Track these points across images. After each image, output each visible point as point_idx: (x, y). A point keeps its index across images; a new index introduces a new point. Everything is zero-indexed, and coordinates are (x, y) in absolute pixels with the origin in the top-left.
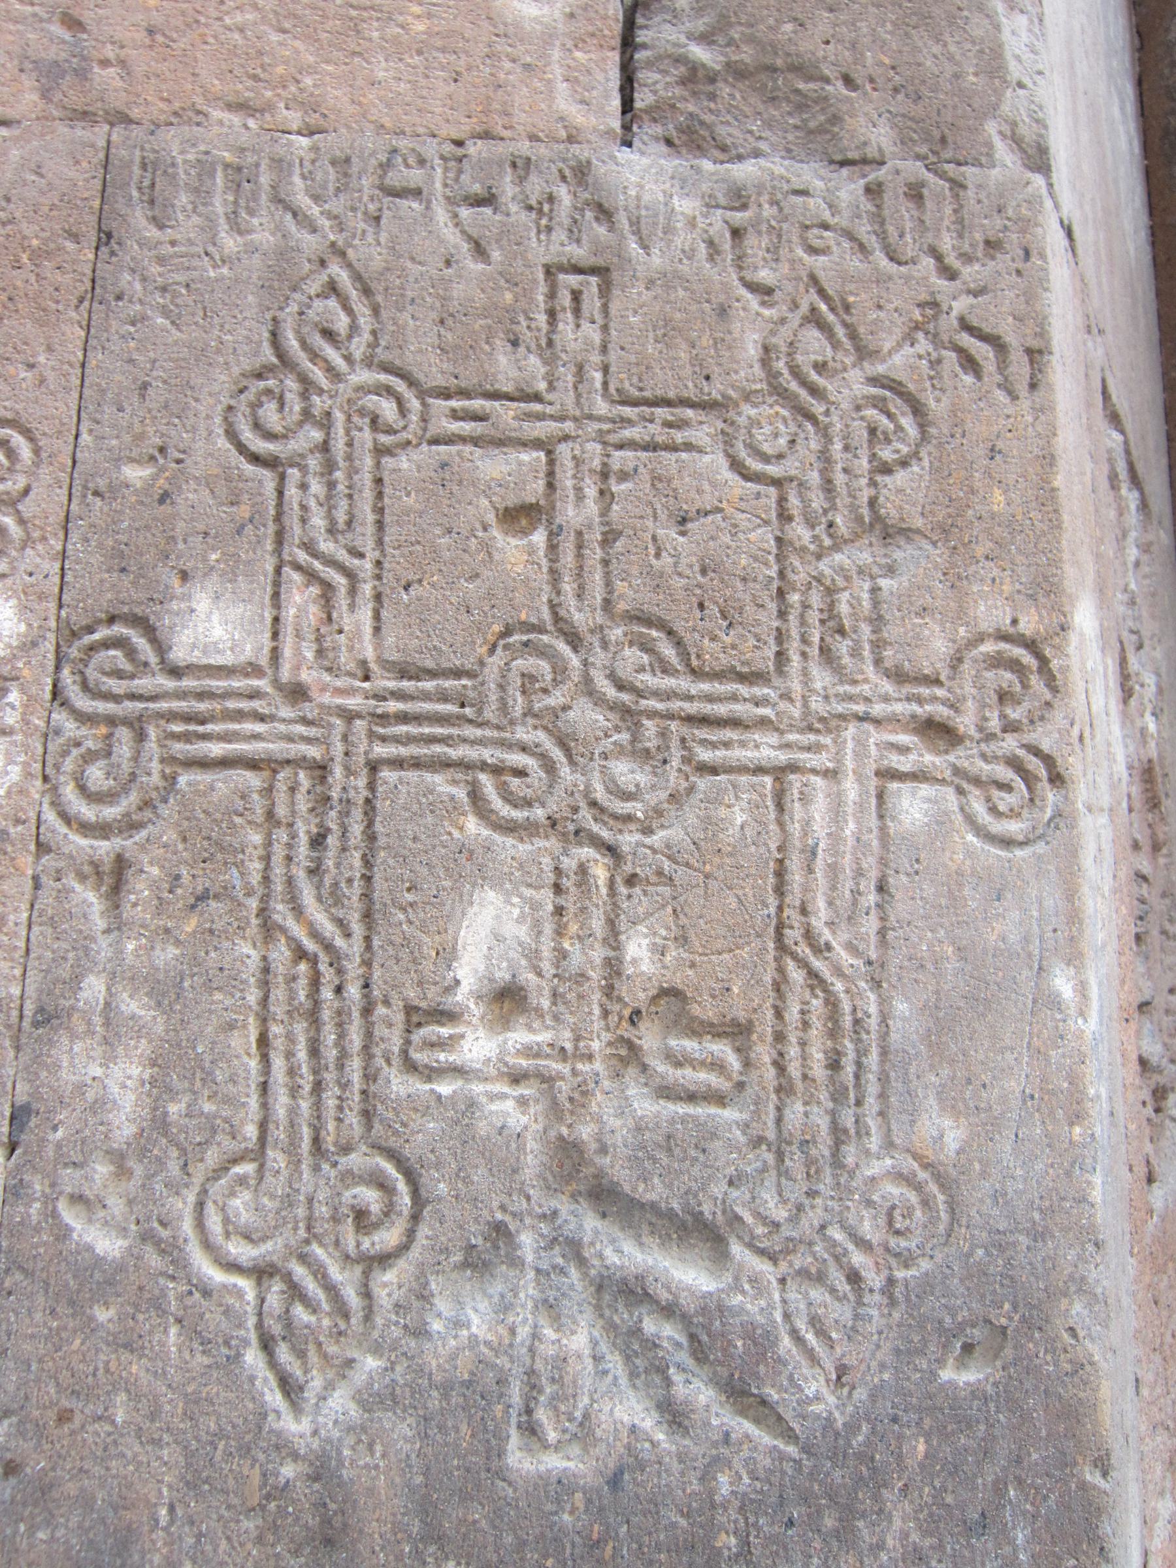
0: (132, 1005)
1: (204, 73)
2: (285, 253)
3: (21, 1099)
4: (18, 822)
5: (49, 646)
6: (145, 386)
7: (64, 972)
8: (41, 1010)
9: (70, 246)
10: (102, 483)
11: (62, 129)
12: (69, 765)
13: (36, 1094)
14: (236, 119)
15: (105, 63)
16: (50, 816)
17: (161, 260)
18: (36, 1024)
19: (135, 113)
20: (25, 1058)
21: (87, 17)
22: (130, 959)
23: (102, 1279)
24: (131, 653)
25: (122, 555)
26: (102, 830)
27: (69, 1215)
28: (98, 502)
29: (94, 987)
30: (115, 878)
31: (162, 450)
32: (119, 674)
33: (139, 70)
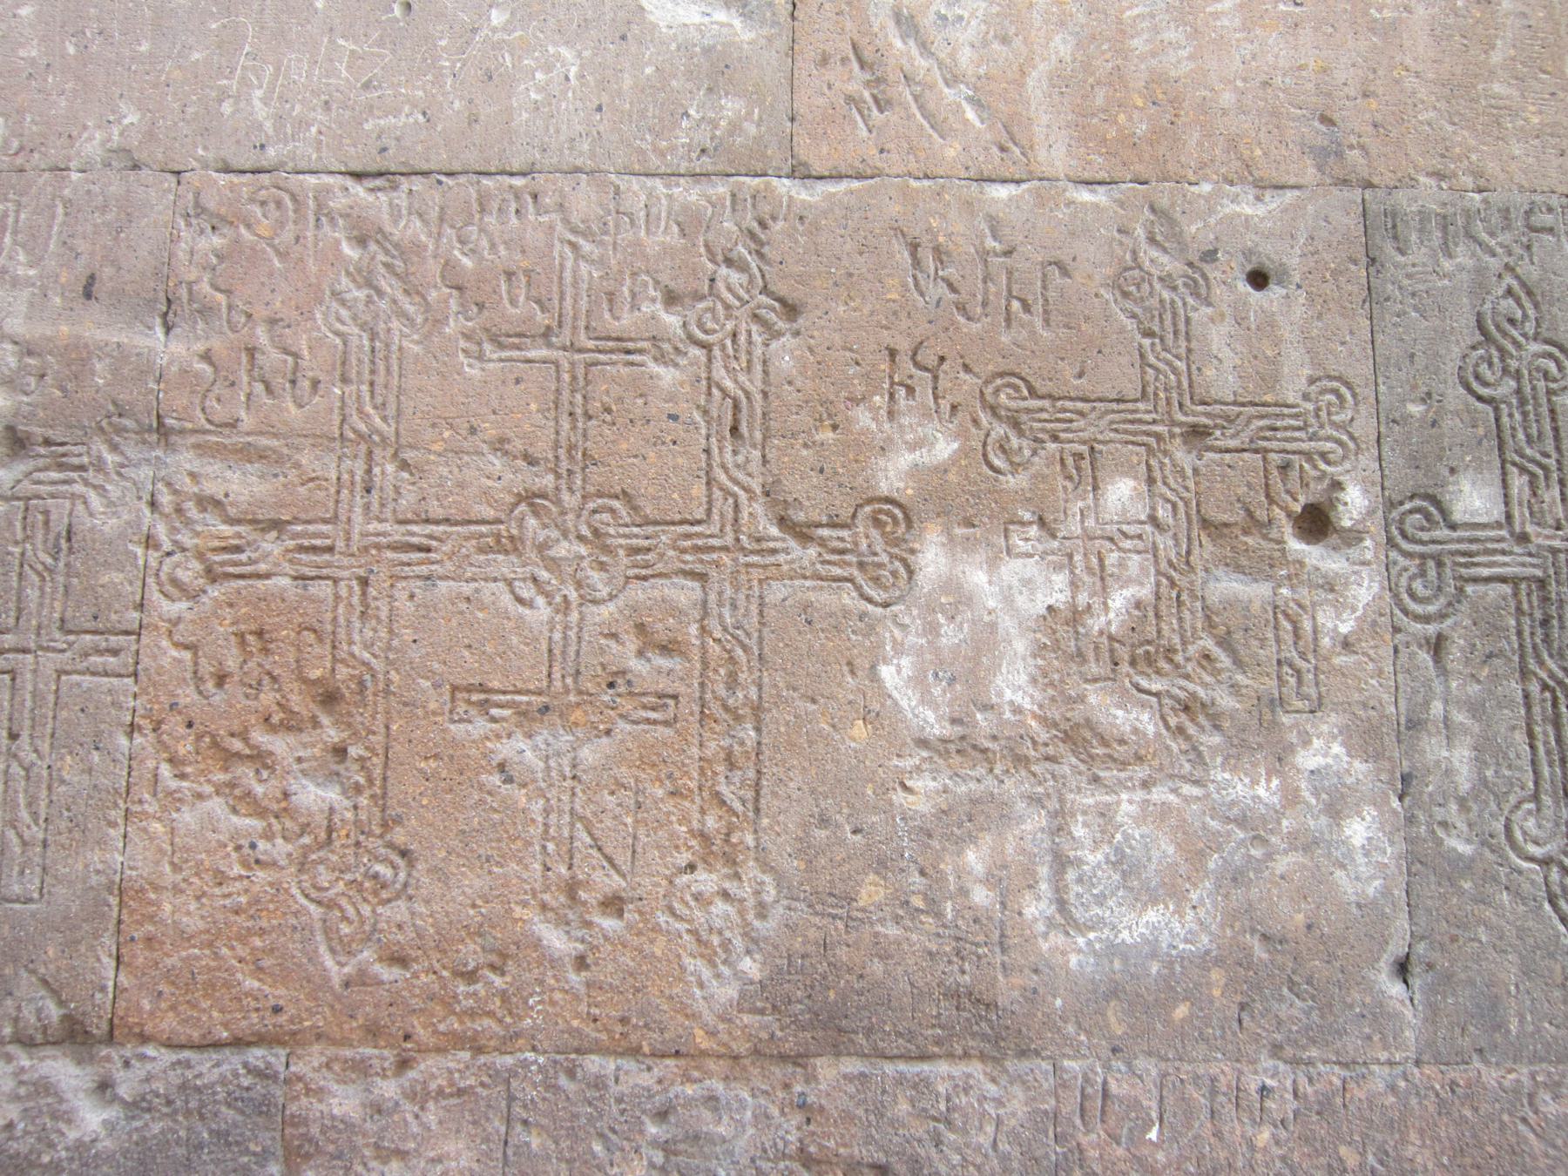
0: (1459, 717)
1: (1412, 154)
2: (1480, 271)
3: (1406, 770)
4: (1381, 615)
5: (1380, 513)
6: (1412, 356)
7: (1420, 699)
8: (1409, 721)
9: (1353, 267)
10: (1397, 415)
11: (1335, 191)
12: (1404, 581)
13: (1413, 767)
14: (1432, 182)
15: (1351, 147)
16: (1397, 611)
17: (1409, 276)
18: (1408, 728)
19: (1376, 180)
20: (1403, 747)
21: (1336, 117)
22: (1455, 692)
23: (1466, 866)
24: (1428, 517)
25: (1415, 458)
26: (1427, 619)
27: (1440, 833)
28: (1397, 428)
29: (1437, 708)
30: (1437, 646)
31: (1429, 394)
32: (1422, 529)
33: (1374, 151)
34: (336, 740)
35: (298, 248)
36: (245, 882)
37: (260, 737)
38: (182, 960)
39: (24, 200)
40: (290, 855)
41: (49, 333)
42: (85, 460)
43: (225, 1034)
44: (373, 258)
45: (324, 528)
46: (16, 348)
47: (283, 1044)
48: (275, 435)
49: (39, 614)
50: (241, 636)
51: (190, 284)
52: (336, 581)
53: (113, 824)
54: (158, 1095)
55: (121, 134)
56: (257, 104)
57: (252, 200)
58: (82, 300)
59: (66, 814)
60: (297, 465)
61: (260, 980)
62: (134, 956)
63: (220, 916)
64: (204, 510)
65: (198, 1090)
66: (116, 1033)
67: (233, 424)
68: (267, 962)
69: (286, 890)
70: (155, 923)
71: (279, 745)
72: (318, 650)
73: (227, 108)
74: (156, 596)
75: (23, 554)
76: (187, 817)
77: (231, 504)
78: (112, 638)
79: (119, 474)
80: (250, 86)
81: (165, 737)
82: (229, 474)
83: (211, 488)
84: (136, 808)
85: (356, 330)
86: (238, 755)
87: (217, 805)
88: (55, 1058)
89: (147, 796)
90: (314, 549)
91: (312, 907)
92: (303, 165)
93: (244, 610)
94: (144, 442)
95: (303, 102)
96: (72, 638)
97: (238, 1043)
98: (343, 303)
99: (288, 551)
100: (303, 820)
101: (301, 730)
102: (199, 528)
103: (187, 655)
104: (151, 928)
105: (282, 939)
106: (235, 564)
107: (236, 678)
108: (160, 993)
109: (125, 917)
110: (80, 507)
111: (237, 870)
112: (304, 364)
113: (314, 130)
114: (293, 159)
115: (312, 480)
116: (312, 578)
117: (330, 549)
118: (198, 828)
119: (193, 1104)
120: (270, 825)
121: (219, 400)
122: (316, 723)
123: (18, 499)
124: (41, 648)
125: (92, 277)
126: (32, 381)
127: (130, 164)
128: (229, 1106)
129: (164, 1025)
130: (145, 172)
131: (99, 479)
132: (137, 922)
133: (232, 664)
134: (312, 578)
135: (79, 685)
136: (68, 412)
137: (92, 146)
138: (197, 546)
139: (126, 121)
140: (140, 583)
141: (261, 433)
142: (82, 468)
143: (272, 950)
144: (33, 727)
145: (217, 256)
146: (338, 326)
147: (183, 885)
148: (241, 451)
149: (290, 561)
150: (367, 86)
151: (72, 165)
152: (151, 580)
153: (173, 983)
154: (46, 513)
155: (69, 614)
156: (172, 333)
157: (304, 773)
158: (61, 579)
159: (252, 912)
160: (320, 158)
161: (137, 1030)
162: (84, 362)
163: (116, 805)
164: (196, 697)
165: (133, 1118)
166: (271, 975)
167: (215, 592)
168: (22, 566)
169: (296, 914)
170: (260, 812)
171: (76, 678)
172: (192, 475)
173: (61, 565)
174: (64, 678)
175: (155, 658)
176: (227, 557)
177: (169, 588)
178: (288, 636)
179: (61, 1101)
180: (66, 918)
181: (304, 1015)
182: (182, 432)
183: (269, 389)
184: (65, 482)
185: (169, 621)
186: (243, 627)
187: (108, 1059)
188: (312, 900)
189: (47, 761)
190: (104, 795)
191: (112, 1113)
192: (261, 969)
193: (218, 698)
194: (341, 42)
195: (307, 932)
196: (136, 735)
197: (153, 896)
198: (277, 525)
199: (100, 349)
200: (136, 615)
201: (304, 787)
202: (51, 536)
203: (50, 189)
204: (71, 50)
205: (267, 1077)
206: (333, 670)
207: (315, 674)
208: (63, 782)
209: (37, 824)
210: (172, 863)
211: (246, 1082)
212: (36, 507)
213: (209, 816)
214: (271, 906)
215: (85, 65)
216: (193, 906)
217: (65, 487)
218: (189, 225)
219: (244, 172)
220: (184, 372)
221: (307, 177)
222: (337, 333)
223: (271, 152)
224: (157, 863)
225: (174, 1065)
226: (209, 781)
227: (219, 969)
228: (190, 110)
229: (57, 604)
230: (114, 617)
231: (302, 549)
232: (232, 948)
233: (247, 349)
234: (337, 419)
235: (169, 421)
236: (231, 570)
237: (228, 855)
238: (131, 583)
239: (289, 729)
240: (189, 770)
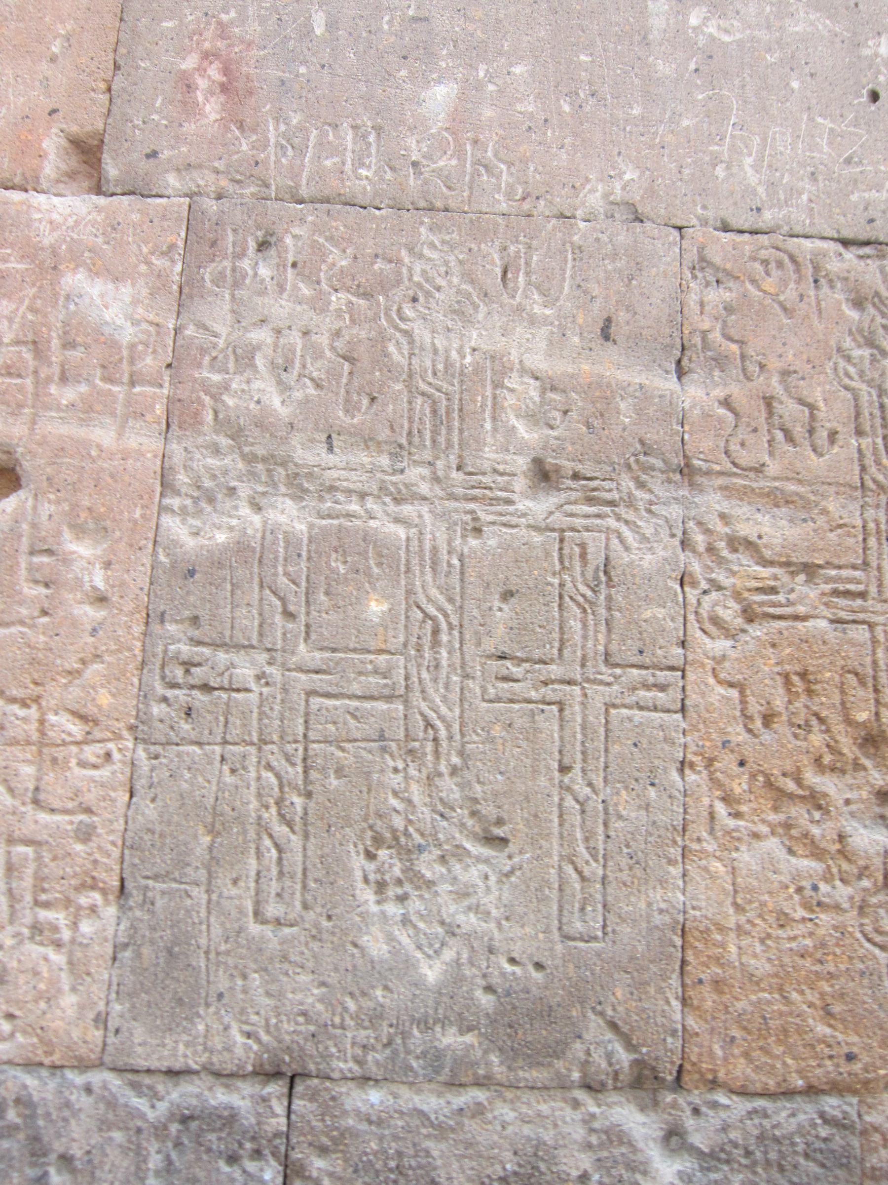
34: (881, 783)
35: (802, 305)
36: (809, 925)
37: (811, 778)
38: (751, 1003)
39: (535, 243)
40: (851, 898)
41: (570, 370)
42: (615, 495)
43: (800, 1082)
44: (872, 320)
45: (857, 574)
46: (538, 383)
47: (855, 1092)
48: (800, 482)
49: (583, 647)
50: (786, 677)
51: (704, 334)
52: (871, 626)
53: (671, 862)
54: (736, 1146)
55: (624, 188)
56: (750, 171)
57: (754, 259)
58: (602, 341)
59: (625, 850)
60: (824, 512)
61: (830, 1026)
62: (703, 999)
63: (786, 960)
64: (735, 550)
65: (777, 1140)
66: (686, 1078)
67: (759, 470)
68: (837, 1008)
69: (850, 933)
70: (722, 965)
71: (827, 784)
72: (861, 692)
73: (720, 171)
74: (699, 633)
75: (562, 585)
76: (745, 857)
77: (766, 546)
78: (658, 673)
79: (650, 511)
80: (741, 153)
81: (718, 774)
82: (759, 516)
83: (745, 530)
84: (695, 846)
85: (864, 387)
86: (791, 796)
87: (773, 844)
88: (619, 1104)
89: (705, 835)
90: (847, 594)
91: (877, 951)
92: (798, 229)
93: (788, 651)
94: (669, 481)
95: (791, 172)
96: (618, 671)
97: (811, 1091)
98: (848, 359)
99: (823, 594)
100: (861, 863)
101: (843, 772)
102: (735, 568)
103: (734, 693)
104: (719, 971)
105: (851, 984)
106: (774, 605)
107: (784, 718)
108: (733, 1039)
109: (690, 958)
110: (615, 541)
111: (801, 913)
112: (821, 415)
113: (805, 197)
114: (788, 223)
115: (840, 526)
116: (847, 622)
117: (863, 595)
118: (759, 869)
119: (773, 1156)
120: (829, 867)
121: (742, 444)
122: (857, 766)
123: (553, 530)
124: (588, 680)
125: (609, 320)
126: (558, 415)
127: (631, 217)
128: (806, 1156)
129: (738, 1073)
130: (648, 225)
131: (630, 515)
132: (704, 964)
133: (779, 703)
134: (847, 622)
135: (630, 719)
136: (596, 448)
137: (594, 199)
138: (734, 585)
139: (627, 177)
140: (681, 619)
141: (788, 479)
142: (611, 503)
143: (842, 995)
144: (584, 761)
145: (725, 309)
146: (847, 381)
147: (748, 927)
148: (768, 495)
149: (826, 604)
150: (848, 161)
151: (579, 213)
152: (691, 617)
153: (745, 1029)
154: (583, 546)
155: (614, 647)
156: (685, 379)
157: (852, 814)
158: (603, 611)
159: (818, 955)
160: (812, 224)
161: (710, 1077)
162: (608, 400)
163: (675, 842)
164: (748, 736)
165: (709, 1169)
166: (843, 1021)
167: (757, 631)
168: (561, 597)
169: (862, 959)
170: (817, 853)
171: (624, 711)
172: (723, 516)
173: (602, 597)
174: (613, 711)
175: (703, 694)
176: (765, 598)
177: (708, 626)
178: (831, 678)
179: (635, 1150)
180: (632, 959)
181: (879, 1063)
182: (708, 473)
183: (789, 438)
184: (598, 516)
185: (714, 658)
186: (788, 667)
187: (674, 1105)
188: (875, 944)
189: (602, 797)
190: (662, 832)
191: (686, 1163)
192: (829, 1014)
193: (767, 737)
194: (820, 120)
195: (875, 977)
196: (687, 771)
197: (719, 937)
198: (810, 570)
199: (623, 389)
200: (680, 651)
201: (856, 829)
202: (590, 569)
203: (559, 235)
204: (567, 108)
205: (845, 1127)
206: (877, 714)
207: (862, 716)
208: (620, 817)
209: (596, 861)
210: (735, 904)
211: (824, 1132)
212: (572, 539)
213: (766, 858)
214: (838, 951)
215: (581, 124)
216: (758, 948)
217: (598, 521)
218: (695, 277)
219: (741, 232)
220: (707, 416)
221: (802, 240)
222: (846, 388)
223: (767, 215)
224: (720, 904)
225: (751, 1113)
226: (763, 821)
227: (791, 1013)
228: (686, 171)
229: (600, 636)
230: (659, 652)
231: (836, 593)
232: (802, 993)
233: (764, 398)
234: (857, 469)
235: (696, 463)
236: (771, 610)
237: (791, 897)
238: (673, 620)
239: (833, 770)
240: (744, 808)
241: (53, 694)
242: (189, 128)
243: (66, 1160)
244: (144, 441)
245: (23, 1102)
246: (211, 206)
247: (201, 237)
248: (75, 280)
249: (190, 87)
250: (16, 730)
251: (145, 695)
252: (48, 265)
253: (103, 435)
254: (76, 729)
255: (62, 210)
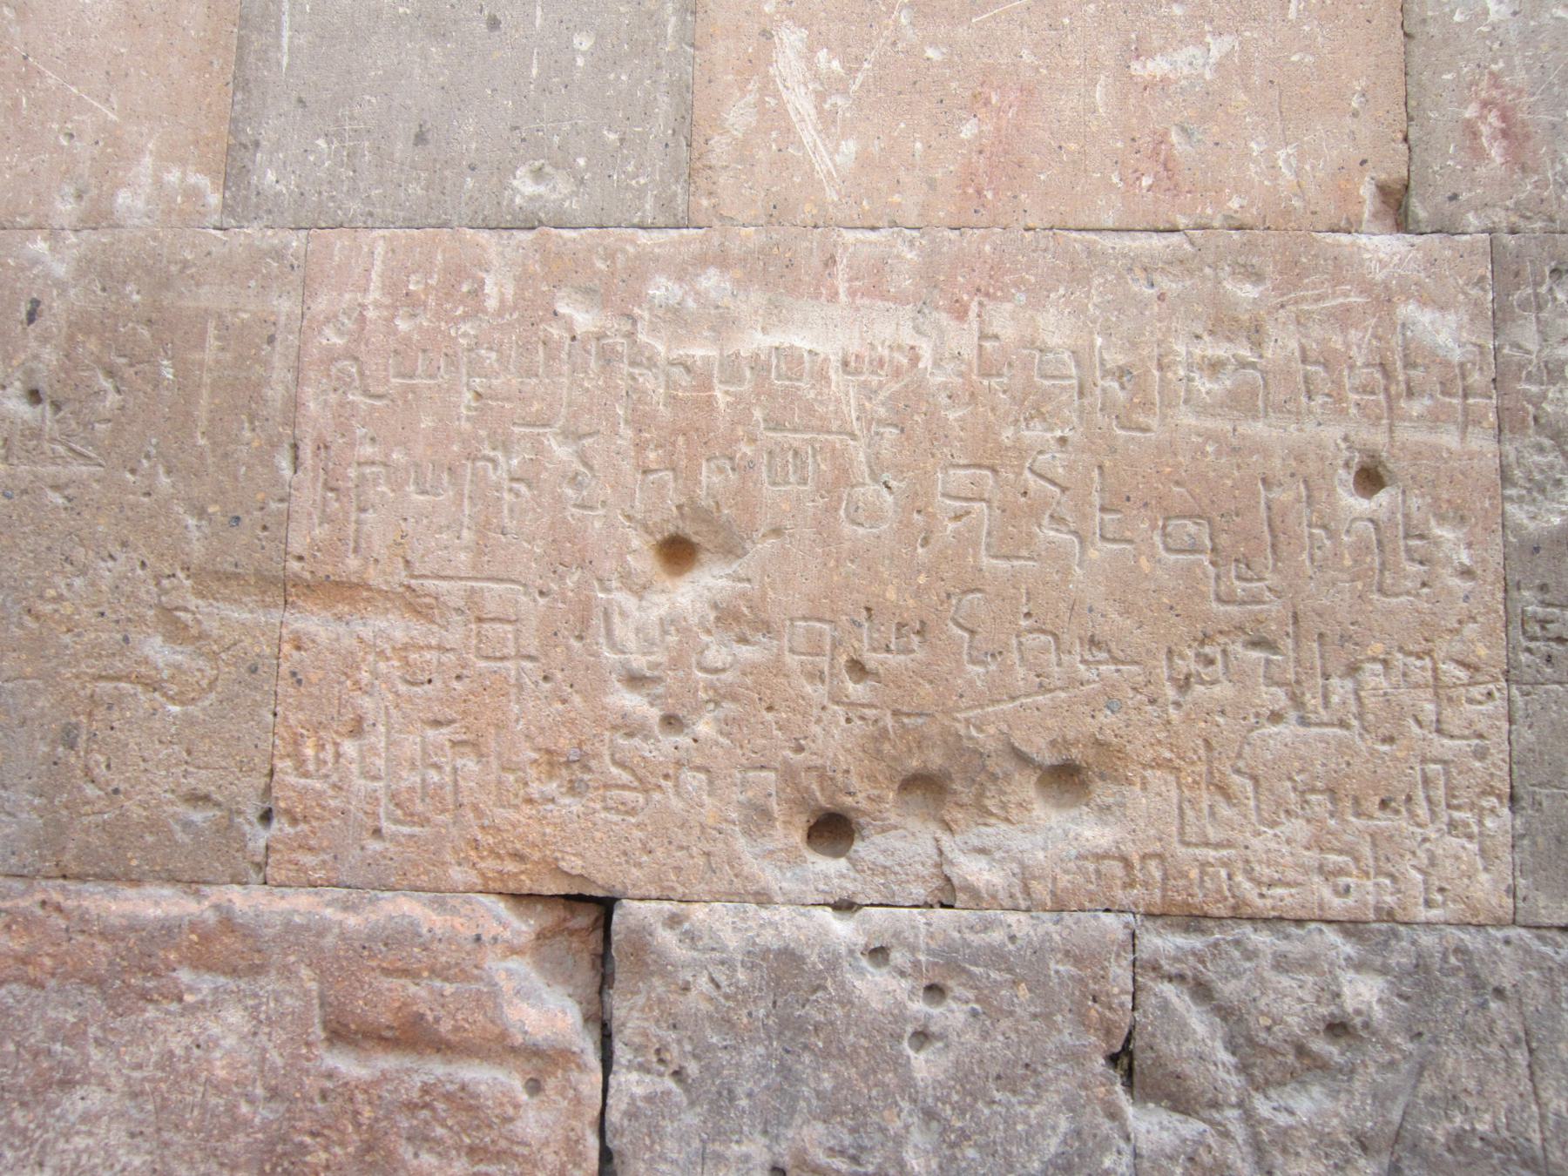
241: (1442, 647)
242: (1481, 171)
243: (1499, 992)
244: (1482, 443)
245: (1460, 950)
246: (1510, 241)
247: (1505, 269)
248: (1407, 310)
249: (1476, 135)
250: (1417, 676)
251: (1512, 648)
252: (1384, 298)
253: (1449, 439)
254: (1463, 674)
255: (1382, 248)
